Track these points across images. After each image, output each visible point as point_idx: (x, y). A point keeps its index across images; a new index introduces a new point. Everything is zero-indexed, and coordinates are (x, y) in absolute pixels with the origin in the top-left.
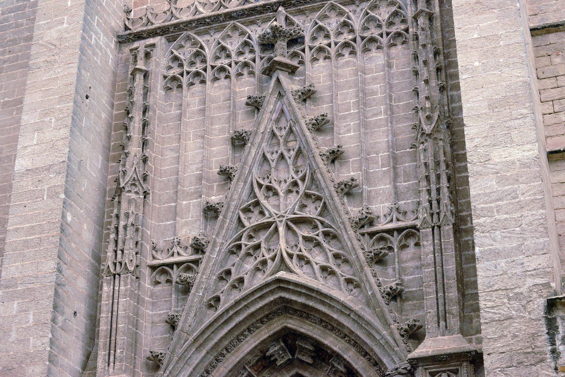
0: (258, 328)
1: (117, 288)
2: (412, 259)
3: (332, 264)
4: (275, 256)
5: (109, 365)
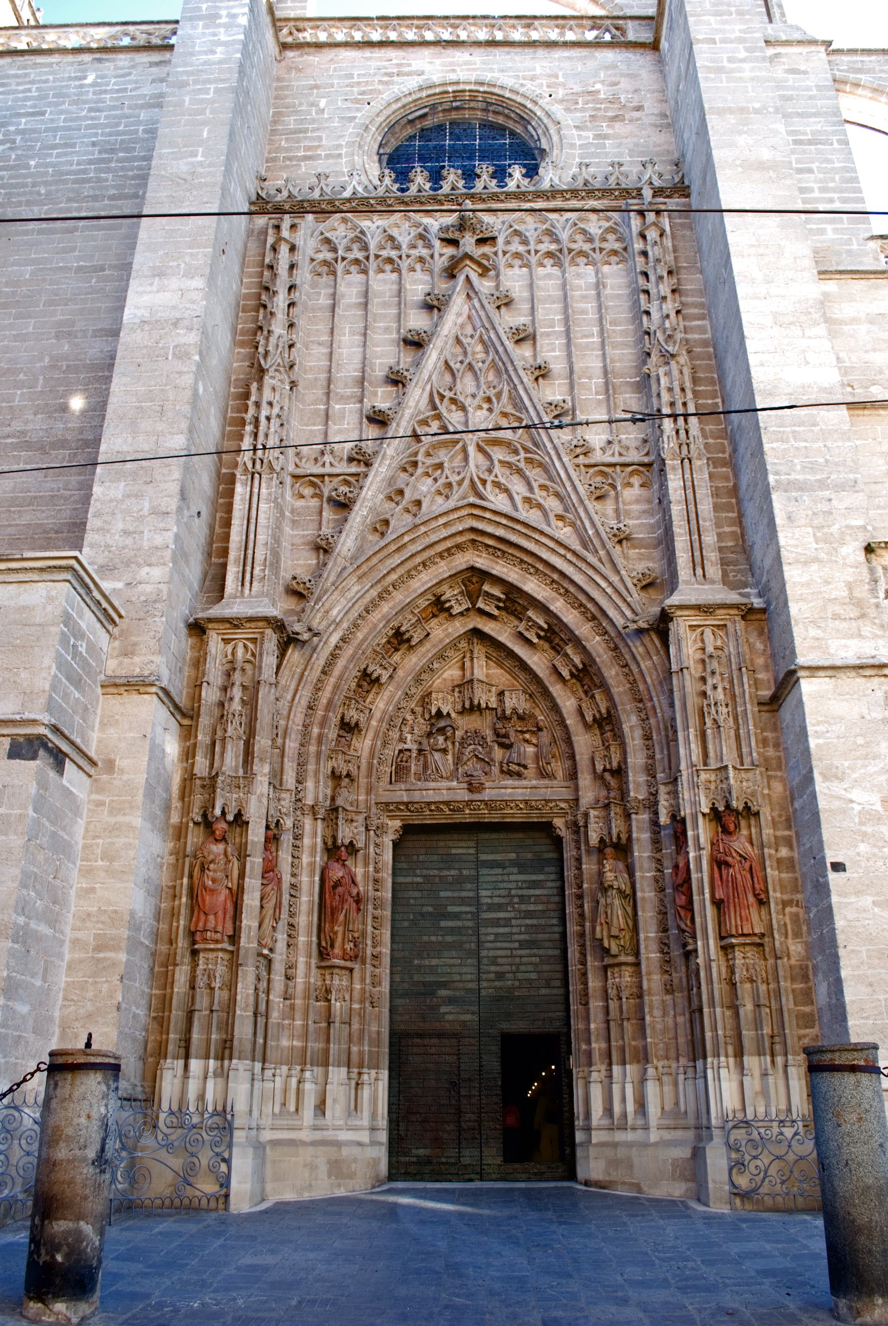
0: (435, 563)
1: (256, 490)
2: (637, 501)
3: (539, 495)
4: (463, 480)
5: (243, 585)
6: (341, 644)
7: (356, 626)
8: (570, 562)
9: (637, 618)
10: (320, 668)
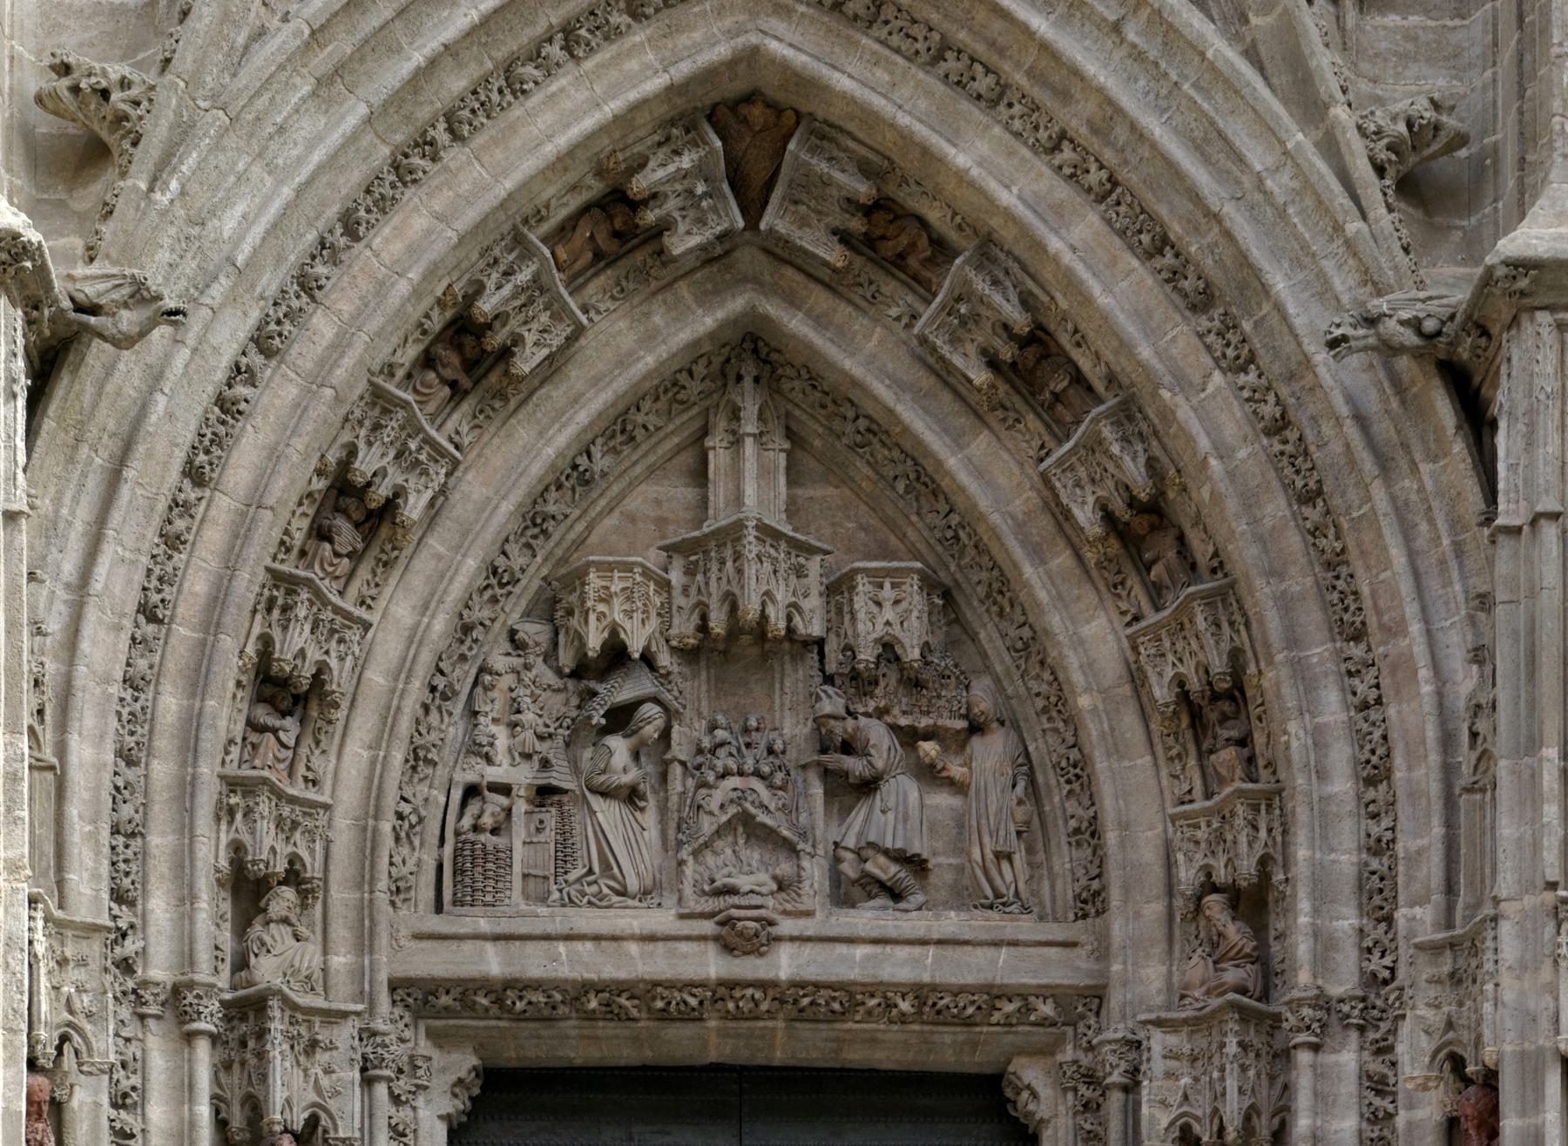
6: (256, 359)
7: (307, 285)
8: (1138, 55)
9: (1381, 305)
10: (180, 456)
